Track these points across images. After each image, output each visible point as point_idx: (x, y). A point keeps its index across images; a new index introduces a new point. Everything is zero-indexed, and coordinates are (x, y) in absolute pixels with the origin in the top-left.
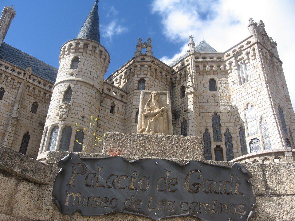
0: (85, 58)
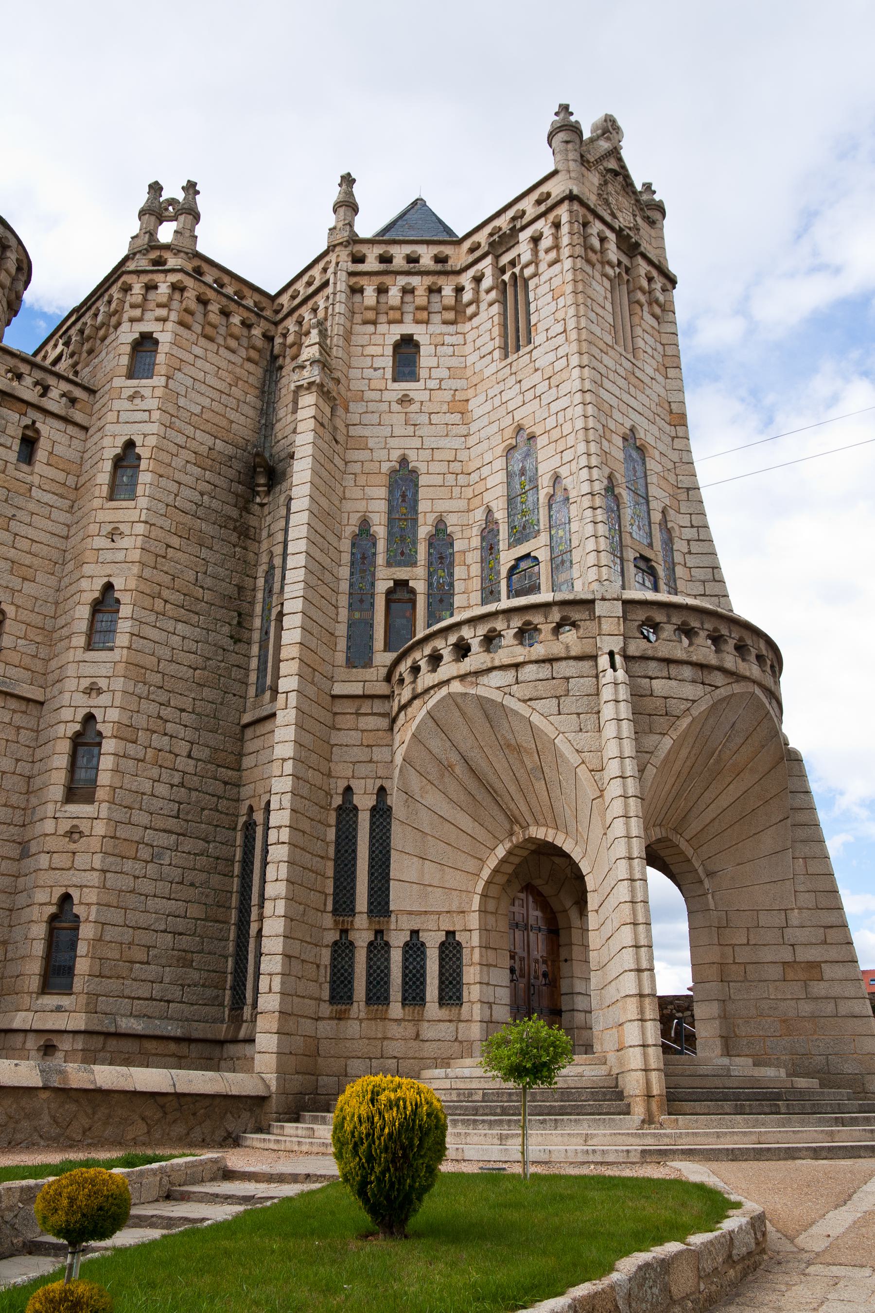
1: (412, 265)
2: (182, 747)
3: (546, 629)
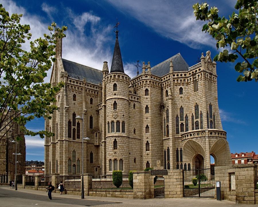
2: (157, 143)
3: (200, 134)
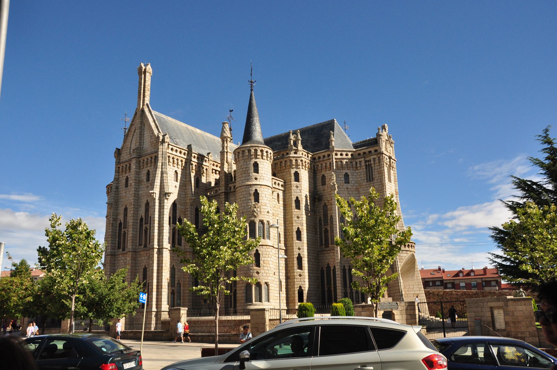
0: (262, 163)
1: (347, 157)
